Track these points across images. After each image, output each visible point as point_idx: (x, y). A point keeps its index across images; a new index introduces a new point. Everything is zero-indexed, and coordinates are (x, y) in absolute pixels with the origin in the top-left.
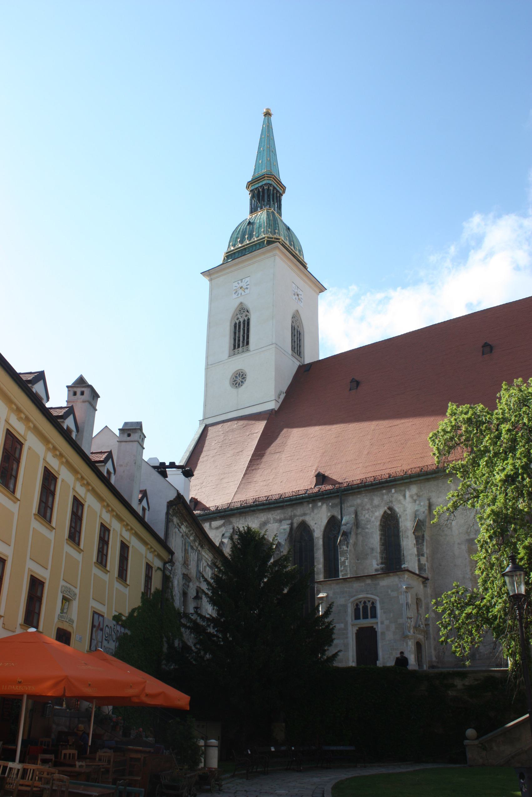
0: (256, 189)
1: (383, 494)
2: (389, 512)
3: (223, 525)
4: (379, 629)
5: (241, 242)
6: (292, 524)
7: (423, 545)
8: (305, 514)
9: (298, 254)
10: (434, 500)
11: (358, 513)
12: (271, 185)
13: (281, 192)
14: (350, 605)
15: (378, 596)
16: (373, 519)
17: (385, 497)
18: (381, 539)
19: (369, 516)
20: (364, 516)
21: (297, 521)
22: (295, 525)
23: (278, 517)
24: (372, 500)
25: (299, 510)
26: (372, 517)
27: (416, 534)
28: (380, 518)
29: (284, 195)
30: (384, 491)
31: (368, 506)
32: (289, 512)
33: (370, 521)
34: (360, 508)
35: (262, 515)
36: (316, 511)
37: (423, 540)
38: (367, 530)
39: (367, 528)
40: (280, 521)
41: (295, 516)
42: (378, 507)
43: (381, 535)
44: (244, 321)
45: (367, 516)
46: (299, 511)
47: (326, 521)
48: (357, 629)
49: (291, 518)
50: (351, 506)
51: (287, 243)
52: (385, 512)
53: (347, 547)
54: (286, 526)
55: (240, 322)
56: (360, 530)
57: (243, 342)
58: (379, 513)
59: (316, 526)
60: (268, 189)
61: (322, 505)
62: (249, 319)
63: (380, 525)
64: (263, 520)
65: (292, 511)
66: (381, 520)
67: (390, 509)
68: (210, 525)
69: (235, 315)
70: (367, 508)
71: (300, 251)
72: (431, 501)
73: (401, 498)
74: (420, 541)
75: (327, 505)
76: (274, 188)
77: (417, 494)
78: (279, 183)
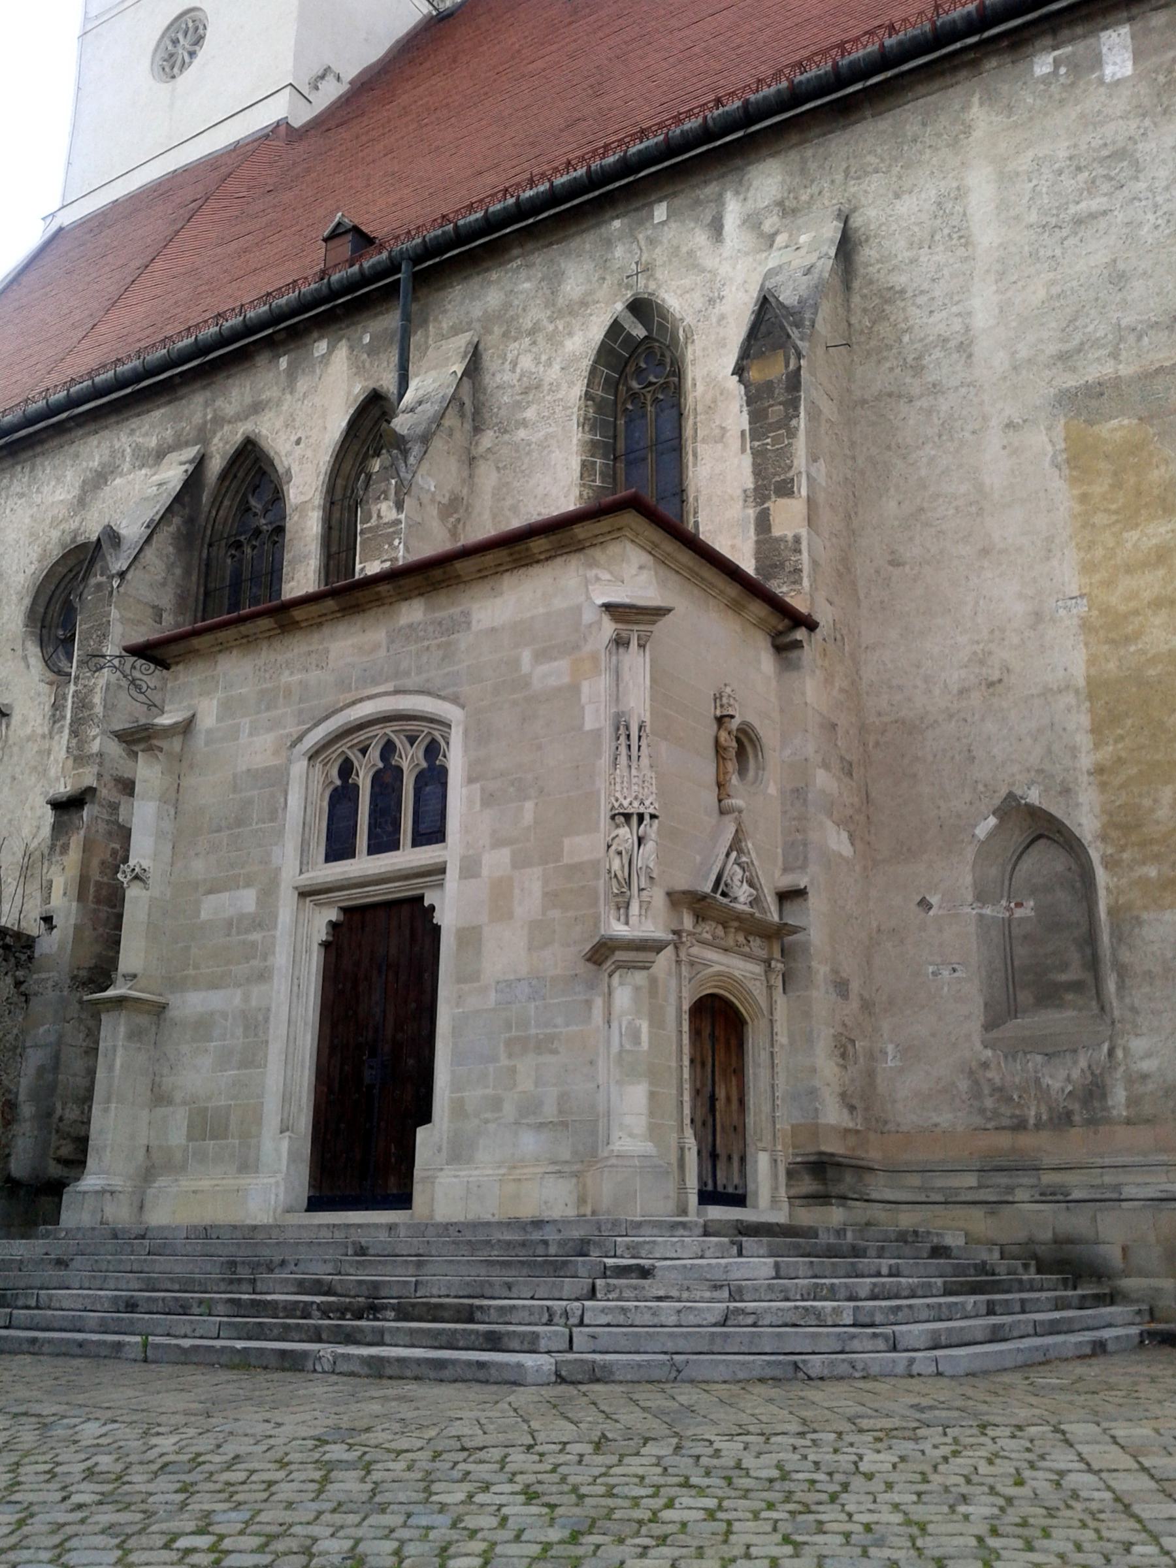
1: (609, 243)
2: (639, 332)
4: (450, 908)
6: (200, 462)
7: (792, 433)
8: (257, 408)
10: (869, 217)
11: (486, 357)
14: (299, 767)
15: (455, 700)
16: (554, 372)
17: (619, 251)
20: (514, 364)
22: (216, 465)
23: (153, 442)
24: (555, 280)
25: (235, 392)
26: (549, 363)
27: (753, 375)
28: (586, 364)
30: (617, 224)
31: (536, 314)
32: (196, 407)
34: (497, 330)
36: (302, 385)
37: (794, 404)
38: (522, 433)
39: (524, 423)
40: (160, 455)
41: (219, 421)
43: (593, 447)
45: (526, 362)
46: (235, 394)
47: (344, 424)
48: (333, 915)
49: (203, 436)
50: (456, 331)
52: (616, 328)
53: (399, 506)
56: (487, 439)
58: (586, 337)
59: (298, 450)
61: (331, 349)
63: (588, 396)
65: (206, 404)
66: (593, 371)
67: (641, 308)
72: (856, 221)
73: (701, 238)
74: (776, 412)
75: (351, 348)
77: (780, 203)
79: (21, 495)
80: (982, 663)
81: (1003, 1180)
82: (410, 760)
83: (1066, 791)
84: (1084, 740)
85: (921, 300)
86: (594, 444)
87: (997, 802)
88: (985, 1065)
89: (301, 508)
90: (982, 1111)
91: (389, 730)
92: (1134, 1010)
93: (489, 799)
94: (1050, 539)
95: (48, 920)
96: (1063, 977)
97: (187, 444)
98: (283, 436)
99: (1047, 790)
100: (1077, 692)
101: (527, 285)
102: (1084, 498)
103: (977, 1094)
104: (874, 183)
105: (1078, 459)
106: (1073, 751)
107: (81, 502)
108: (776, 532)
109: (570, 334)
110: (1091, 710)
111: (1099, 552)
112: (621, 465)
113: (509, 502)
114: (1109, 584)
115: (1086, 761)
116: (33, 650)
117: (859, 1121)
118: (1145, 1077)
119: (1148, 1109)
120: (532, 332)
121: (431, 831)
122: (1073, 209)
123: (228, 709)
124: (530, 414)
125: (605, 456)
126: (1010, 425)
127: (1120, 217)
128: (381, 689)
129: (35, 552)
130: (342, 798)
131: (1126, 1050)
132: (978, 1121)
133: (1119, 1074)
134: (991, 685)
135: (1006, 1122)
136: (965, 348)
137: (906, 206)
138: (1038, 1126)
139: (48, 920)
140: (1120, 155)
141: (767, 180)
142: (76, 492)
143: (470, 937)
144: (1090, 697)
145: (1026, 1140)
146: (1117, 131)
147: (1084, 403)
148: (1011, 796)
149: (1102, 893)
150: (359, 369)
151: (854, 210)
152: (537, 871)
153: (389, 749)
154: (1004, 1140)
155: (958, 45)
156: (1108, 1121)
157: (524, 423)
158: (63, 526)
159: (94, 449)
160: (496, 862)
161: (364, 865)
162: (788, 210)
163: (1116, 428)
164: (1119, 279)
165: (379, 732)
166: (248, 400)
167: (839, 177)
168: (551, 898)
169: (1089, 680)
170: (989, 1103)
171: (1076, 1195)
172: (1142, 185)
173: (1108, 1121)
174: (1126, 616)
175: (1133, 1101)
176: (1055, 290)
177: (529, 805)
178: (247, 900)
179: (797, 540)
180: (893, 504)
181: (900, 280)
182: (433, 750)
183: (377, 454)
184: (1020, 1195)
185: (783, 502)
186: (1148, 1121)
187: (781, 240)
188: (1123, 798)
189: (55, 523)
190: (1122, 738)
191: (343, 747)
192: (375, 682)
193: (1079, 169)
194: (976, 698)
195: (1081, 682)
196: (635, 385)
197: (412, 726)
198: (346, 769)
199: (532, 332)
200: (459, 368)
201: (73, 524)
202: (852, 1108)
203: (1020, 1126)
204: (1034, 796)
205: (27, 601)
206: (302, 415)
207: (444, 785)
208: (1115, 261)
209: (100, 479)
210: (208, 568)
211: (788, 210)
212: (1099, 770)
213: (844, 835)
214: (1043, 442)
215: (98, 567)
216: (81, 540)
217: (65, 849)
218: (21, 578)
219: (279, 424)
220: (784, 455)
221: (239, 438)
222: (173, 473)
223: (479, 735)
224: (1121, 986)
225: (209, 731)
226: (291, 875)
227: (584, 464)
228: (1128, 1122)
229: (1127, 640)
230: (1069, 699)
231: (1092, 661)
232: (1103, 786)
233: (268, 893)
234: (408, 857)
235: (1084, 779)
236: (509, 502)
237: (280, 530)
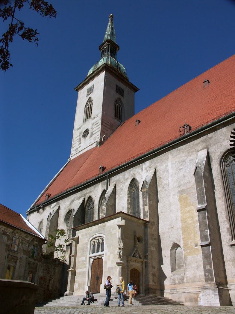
1: (130, 171)
7: (147, 198)
8: (91, 192)
17: (131, 172)
18: (128, 200)
19: (123, 186)
20: (120, 186)
23: (79, 196)
24: (124, 175)
26: (124, 186)
27: (143, 191)
28: (128, 186)
32: (84, 191)
33: (123, 189)
36: (96, 189)
39: (121, 194)
40: (80, 198)
41: (87, 193)
42: (127, 179)
43: (129, 197)
45: (121, 186)
46: (89, 190)
49: (85, 196)
50: (114, 182)
59: (96, 197)
63: (128, 191)
64: (72, 199)
69: (87, 104)
70: (121, 181)
73: (140, 170)
77: (149, 166)
79: (64, 203)
80: (171, 225)
81: (173, 291)
82: (101, 241)
83: (180, 241)
84: (181, 235)
85: (164, 179)
86: (129, 197)
87: (172, 243)
88: (171, 276)
89: (96, 205)
90: (171, 282)
91: (98, 238)
92: (187, 269)
93: (108, 246)
94: (178, 209)
96: (181, 265)
97: (83, 196)
98: (94, 196)
99: (178, 241)
100: (180, 229)
101: (121, 176)
102: (181, 204)
103: (170, 280)
104: (159, 164)
105: (180, 199)
106: (180, 236)
107: (71, 204)
108: (145, 210)
109: (126, 183)
110: (182, 231)
111: (183, 211)
112: (133, 199)
113: (119, 204)
114: (184, 215)
115: (182, 237)
117: (156, 284)
118: (188, 277)
119: (188, 281)
120: (122, 182)
121: (102, 250)
122: (179, 168)
123: (83, 235)
124: (122, 193)
125: (130, 198)
126: (173, 195)
127: (184, 169)
128: (98, 233)
129: (65, 210)
130: (94, 246)
131: (186, 274)
132: (171, 283)
133: (185, 277)
134: (172, 228)
135: (174, 283)
136: (168, 185)
137: (162, 167)
138: (177, 284)
140: (184, 161)
141: (147, 163)
142: (70, 203)
143: (106, 262)
144: (182, 229)
145: (175, 285)
146: (184, 158)
147: (181, 192)
148: (174, 242)
149: (183, 254)
150: (102, 186)
151: (157, 167)
152: (112, 255)
153: (99, 240)
154: (173, 286)
155: (166, 148)
156: (184, 283)
157: (121, 194)
158: (69, 207)
159: (72, 197)
160: (108, 254)
161: (96, 254)
162: (150, 167)
163: (184, 195)
164: (184, 177)
165: (97, 238)
166: (90, 191)
167: (155, 163)
168: (113, 258)
169: (182, 227)
170: (172, 281)
171: (180, 292)
172: (186, 165)
173: (184, 283)
174: (185, 219)
175: (187, 280)
176: (178, 178)
177: (111, 247)
178: (84, 258)
179: (148, 211)
180: (161, 205)
181: (161, 176)
182: (103, 240)
183: (102, 200)
184: (175, 293)
185: (146, 207)
186: (188, 283)
187: (149, 171)
188: (185, 242)
189: (68, 207)
190: (185, 234)
191: (94, 240)
192: (97, 232)
193: (180, 163)
194: (170, 230)
195: (181, 227)
196: (134, 189)
197: (101, 237)
198: (94, 242)
199: (122, 182)
200: (113, 187)
202: (155, 283)
203: (175, 284)
204: (176, 242)
205: (64, 217)
206: (96, 192)
207: (104, 244)
208: (184, 174)
209: (72, 201)
211: (150, 167)
212: (183, 238)
213: (154, 248)
214: (176, 197)
215: (71, 214)
216: (70, 209)
217: (68, 251)
218: (64, 214)
219: (94, 194)
220: (146, 200)
221: (89, 196)
222: (81, 201)
223: (107, 239)
224: (185, 265)
225: (81, 238)
226: (89, 256)
227: (128, 199)
228: (186, 283)
229: (186, 222)
230: (180, 229)
231: (182, 225)
232: (183, 241)
233: (86, 258)
234: (100, 253)
235: (181, 240)
236: (119, 204)
237: (94, 207)
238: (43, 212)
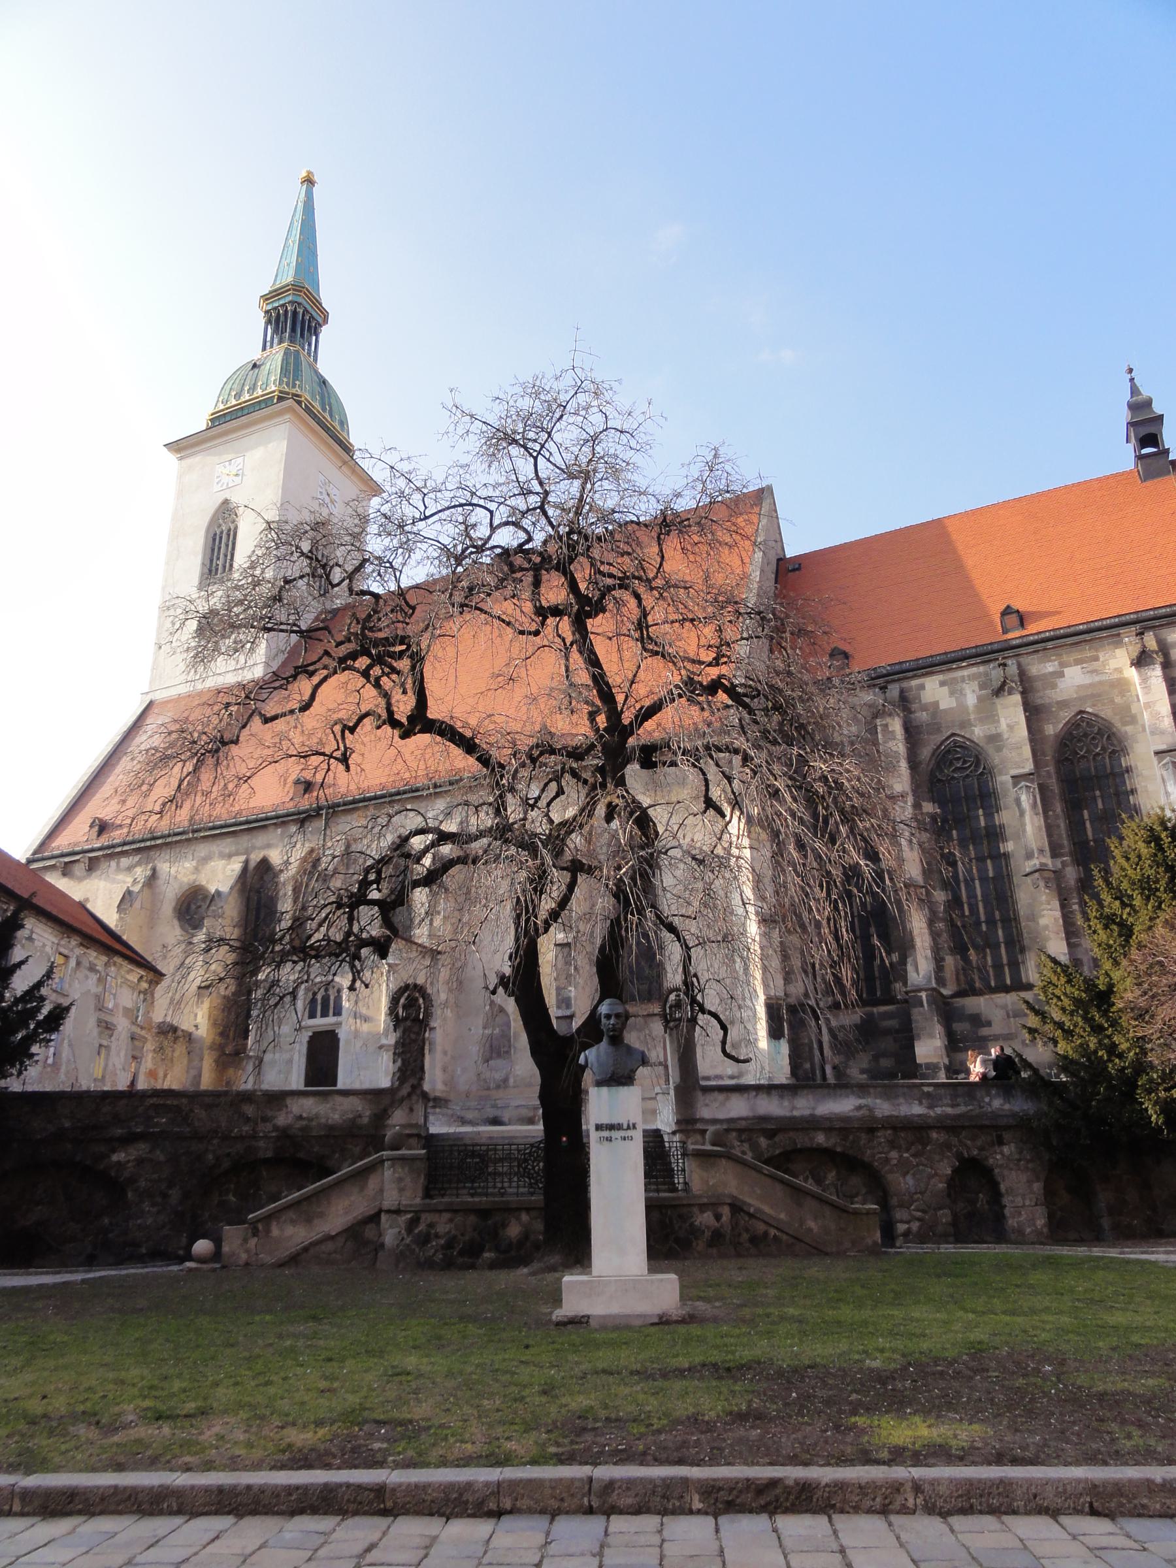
0: (275, 308)
3: (139, 864)
5: (238, 396)
6: (247, 862)
8: (269, 846)
9: (338, 428)
12: (299, 304)
13: (320, 321)
21: (256, 857)
22: (252, 865)
23: (227, 851)
29: (324, 328)
32: (244, 841)
35: (202, 846)
40: (230, 856)
41: (254, 848)
44: (229, 530)
46: (260, 839)
49: (247, 852)
51: (317, 405)
54: (236, 866)
55: (222, 533)
57: (224, 567)
60: (295, 313)
62: (236, 528)
68: (118, 863)
71: (343, 423)
76: (306, 311)
78: (317, 303)
95: (196, 1026)
116: (176, 922)
139: (196, 1026)
201: (193, 877)
209: (206, 860)
210: (248, 899)
221: (261, 856)
238: (89, 876)
